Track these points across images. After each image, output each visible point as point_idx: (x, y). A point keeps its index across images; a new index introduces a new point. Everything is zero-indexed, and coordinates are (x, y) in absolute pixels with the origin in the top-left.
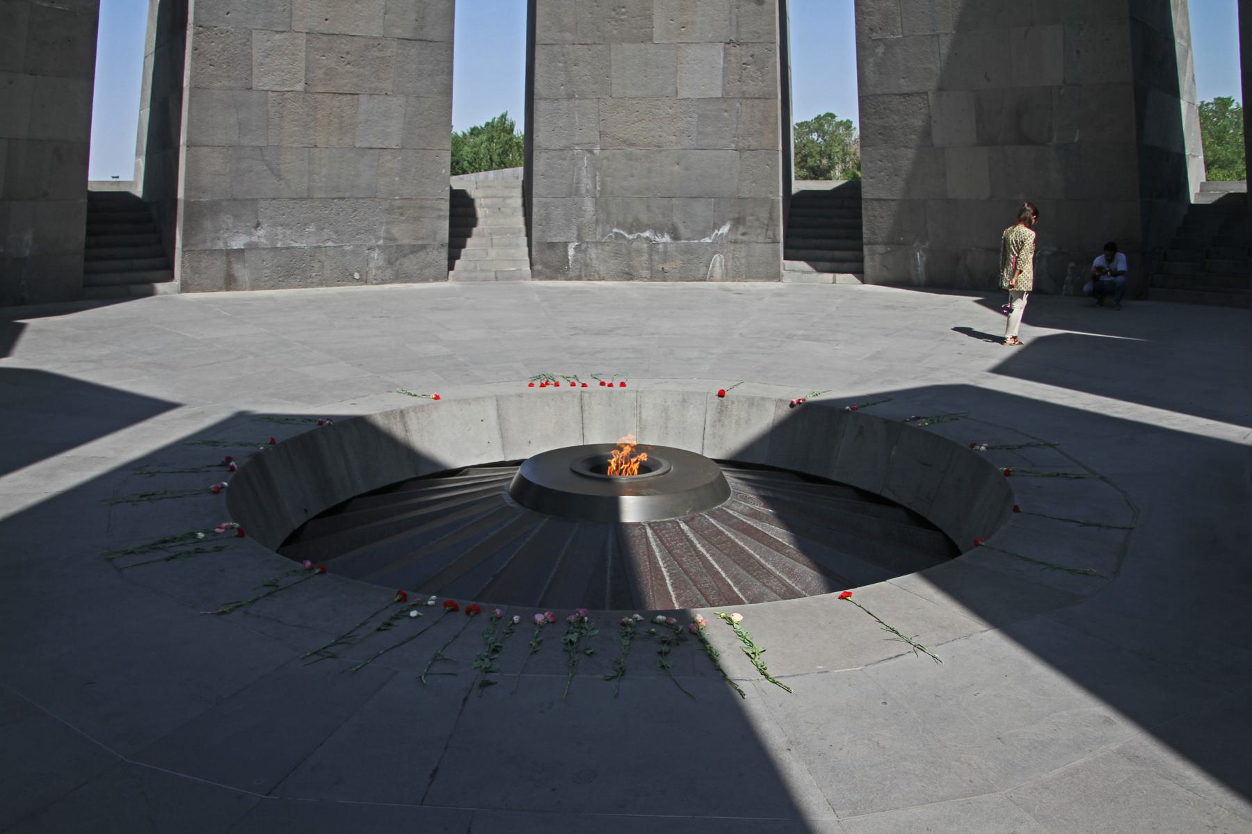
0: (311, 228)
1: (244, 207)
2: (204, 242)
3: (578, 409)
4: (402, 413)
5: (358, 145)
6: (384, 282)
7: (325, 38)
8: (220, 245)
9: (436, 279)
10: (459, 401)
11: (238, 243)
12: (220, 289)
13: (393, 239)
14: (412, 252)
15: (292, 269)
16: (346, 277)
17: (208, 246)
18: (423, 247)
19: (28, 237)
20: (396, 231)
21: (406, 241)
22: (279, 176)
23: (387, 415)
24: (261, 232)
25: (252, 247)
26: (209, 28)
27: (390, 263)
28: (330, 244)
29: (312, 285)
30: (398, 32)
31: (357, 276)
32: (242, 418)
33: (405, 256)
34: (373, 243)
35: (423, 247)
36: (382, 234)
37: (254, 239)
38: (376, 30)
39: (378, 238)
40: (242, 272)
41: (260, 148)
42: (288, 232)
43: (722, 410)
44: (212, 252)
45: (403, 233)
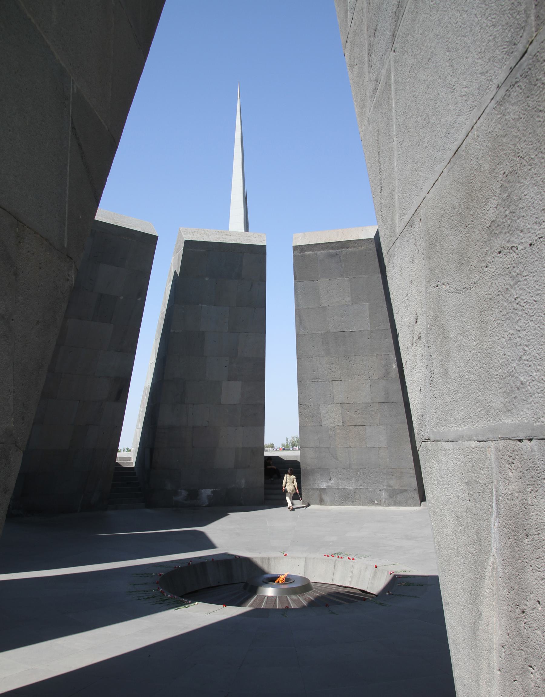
0: (353, 481)
1: (325, 471)
2: (310, 485)
3: (333, 566)
4: (269, 559)
5: (368, 446)
6: (389, 505)
7: (348, 405)
8: (316, 486)
9: (415, 505)
10: (292, 558)
11: (323, 485)
12: (318, 505)
13: (391, 486)
14: (401, 493)
15: (347, 497)
16: (371, 502)
17: (311, 486)
18: (406, 490)
19: (243, 481)
20: (392, 482)
21: (397, 488)
22: (337, 459)
23: (262, 559)
24: (332, 482)
25: (329, 488)
26: (303, 405)
27: (391, 497)
28: (362, 487)
29: (356, 505)
31: (376, 502)
32: (225, 554)
33: (397, 494)
34: (381, 487)
35: (406, 490)
36: (385, 484)
37: (330, 484)
39: (383, 486)
40: (326, 497)
41: (328, 448)
42: (344, 482)
43: (375, 573)
44: (313, 489)
45: (395, 483)
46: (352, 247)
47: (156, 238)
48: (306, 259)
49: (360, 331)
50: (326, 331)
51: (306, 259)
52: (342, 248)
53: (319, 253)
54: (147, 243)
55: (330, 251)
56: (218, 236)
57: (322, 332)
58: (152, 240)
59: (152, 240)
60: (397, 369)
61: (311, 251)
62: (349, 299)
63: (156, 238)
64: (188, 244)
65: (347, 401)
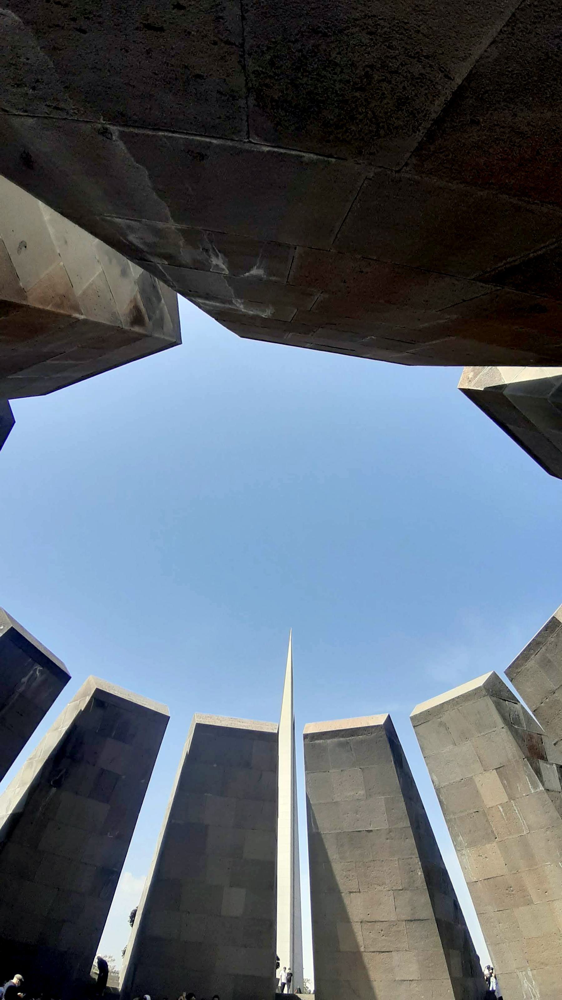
30: (404, 917)
38: (393, 917)
46: (362, 735)
47: (166, 719)
48: (316, 746)
49: (378, 830)
50: (339, 831)
51: (316, 746)
52: (352, 736)
53: (329, 741)
54: (158, 722)
55: (342, 739)
56: (230, 722)
57: (337, 831)
58: (161, 721)
59: (161, 721)
60: (423, 876)
61: (321, 739)
62: (362, 792)
63: (166, 719)
64: (200, 729)
65: (368, 918)
